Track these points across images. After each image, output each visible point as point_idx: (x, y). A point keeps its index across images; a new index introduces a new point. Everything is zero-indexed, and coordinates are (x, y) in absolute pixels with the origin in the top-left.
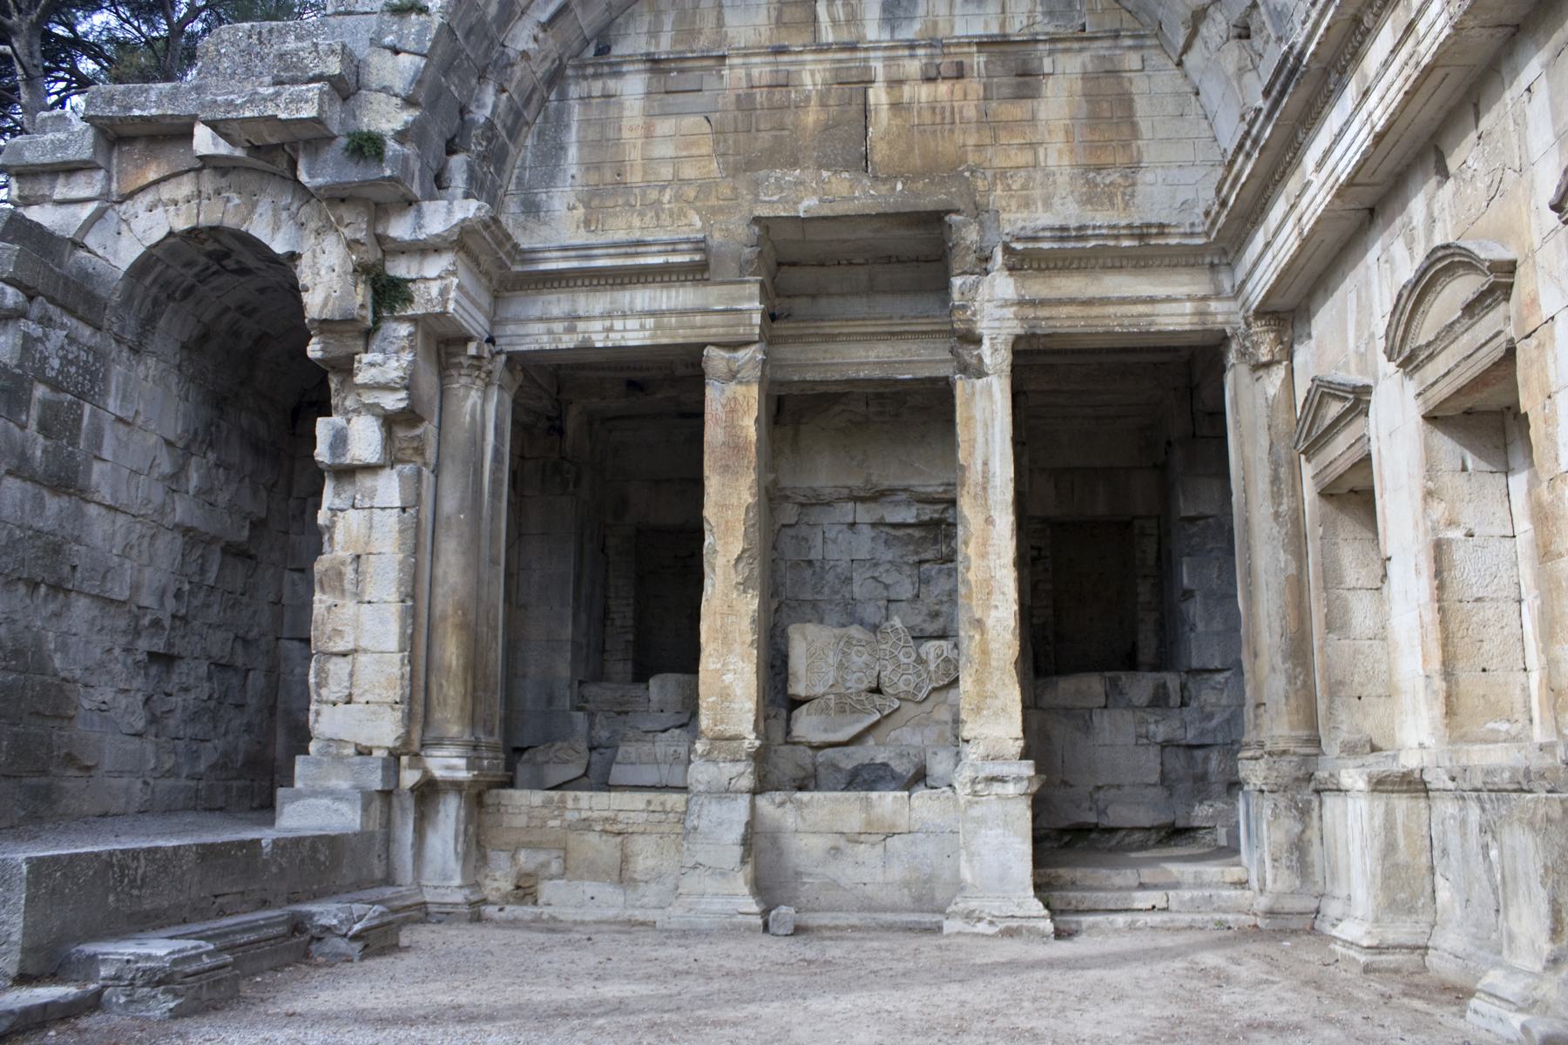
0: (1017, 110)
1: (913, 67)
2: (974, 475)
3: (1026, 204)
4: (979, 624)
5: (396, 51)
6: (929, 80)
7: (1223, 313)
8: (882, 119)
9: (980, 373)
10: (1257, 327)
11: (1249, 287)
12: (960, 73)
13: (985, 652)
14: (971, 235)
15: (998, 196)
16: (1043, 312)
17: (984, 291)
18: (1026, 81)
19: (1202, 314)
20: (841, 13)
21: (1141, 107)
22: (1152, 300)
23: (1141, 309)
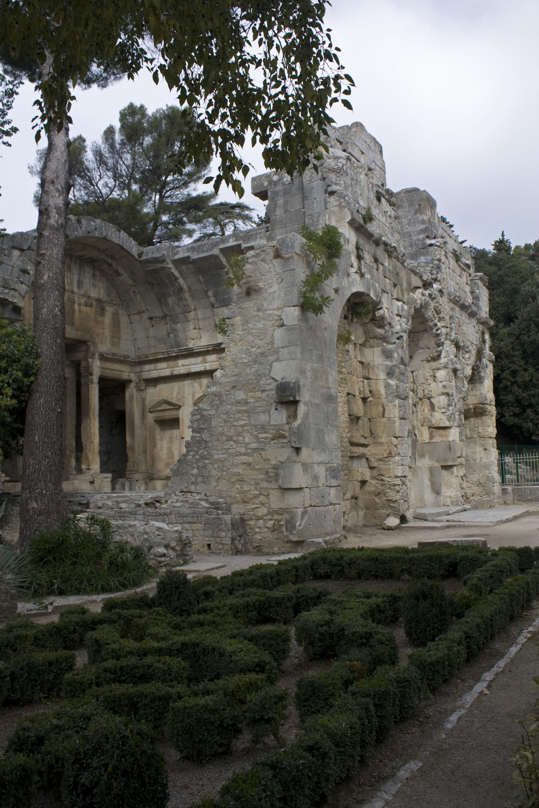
0: (100, 318)
1: (83, 301)
2: (92, 408)
3: (102, 343)
4: (93, 442)
5: (22, 283)
6: (86, 306)
7: (133, 377)
8: (77, 313)
9: (92, 383)
10: (142, 382)
11: (143, 374)
12: (91, 306)
13: (94, 449)
14: (92, 349)
15: (97, 340)
16: (105, 371)
17: (94, 363)
18: (102, 312)
19: (129, 376)
20: (69, 281)
21: (122, 324)
22: (122, 371)
23: (120, 373)
